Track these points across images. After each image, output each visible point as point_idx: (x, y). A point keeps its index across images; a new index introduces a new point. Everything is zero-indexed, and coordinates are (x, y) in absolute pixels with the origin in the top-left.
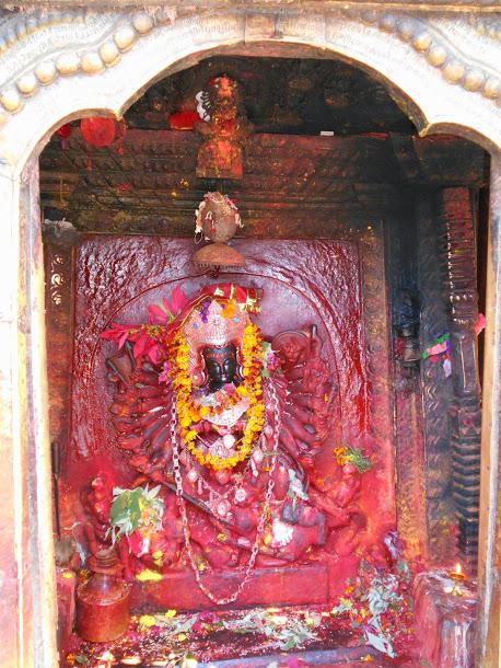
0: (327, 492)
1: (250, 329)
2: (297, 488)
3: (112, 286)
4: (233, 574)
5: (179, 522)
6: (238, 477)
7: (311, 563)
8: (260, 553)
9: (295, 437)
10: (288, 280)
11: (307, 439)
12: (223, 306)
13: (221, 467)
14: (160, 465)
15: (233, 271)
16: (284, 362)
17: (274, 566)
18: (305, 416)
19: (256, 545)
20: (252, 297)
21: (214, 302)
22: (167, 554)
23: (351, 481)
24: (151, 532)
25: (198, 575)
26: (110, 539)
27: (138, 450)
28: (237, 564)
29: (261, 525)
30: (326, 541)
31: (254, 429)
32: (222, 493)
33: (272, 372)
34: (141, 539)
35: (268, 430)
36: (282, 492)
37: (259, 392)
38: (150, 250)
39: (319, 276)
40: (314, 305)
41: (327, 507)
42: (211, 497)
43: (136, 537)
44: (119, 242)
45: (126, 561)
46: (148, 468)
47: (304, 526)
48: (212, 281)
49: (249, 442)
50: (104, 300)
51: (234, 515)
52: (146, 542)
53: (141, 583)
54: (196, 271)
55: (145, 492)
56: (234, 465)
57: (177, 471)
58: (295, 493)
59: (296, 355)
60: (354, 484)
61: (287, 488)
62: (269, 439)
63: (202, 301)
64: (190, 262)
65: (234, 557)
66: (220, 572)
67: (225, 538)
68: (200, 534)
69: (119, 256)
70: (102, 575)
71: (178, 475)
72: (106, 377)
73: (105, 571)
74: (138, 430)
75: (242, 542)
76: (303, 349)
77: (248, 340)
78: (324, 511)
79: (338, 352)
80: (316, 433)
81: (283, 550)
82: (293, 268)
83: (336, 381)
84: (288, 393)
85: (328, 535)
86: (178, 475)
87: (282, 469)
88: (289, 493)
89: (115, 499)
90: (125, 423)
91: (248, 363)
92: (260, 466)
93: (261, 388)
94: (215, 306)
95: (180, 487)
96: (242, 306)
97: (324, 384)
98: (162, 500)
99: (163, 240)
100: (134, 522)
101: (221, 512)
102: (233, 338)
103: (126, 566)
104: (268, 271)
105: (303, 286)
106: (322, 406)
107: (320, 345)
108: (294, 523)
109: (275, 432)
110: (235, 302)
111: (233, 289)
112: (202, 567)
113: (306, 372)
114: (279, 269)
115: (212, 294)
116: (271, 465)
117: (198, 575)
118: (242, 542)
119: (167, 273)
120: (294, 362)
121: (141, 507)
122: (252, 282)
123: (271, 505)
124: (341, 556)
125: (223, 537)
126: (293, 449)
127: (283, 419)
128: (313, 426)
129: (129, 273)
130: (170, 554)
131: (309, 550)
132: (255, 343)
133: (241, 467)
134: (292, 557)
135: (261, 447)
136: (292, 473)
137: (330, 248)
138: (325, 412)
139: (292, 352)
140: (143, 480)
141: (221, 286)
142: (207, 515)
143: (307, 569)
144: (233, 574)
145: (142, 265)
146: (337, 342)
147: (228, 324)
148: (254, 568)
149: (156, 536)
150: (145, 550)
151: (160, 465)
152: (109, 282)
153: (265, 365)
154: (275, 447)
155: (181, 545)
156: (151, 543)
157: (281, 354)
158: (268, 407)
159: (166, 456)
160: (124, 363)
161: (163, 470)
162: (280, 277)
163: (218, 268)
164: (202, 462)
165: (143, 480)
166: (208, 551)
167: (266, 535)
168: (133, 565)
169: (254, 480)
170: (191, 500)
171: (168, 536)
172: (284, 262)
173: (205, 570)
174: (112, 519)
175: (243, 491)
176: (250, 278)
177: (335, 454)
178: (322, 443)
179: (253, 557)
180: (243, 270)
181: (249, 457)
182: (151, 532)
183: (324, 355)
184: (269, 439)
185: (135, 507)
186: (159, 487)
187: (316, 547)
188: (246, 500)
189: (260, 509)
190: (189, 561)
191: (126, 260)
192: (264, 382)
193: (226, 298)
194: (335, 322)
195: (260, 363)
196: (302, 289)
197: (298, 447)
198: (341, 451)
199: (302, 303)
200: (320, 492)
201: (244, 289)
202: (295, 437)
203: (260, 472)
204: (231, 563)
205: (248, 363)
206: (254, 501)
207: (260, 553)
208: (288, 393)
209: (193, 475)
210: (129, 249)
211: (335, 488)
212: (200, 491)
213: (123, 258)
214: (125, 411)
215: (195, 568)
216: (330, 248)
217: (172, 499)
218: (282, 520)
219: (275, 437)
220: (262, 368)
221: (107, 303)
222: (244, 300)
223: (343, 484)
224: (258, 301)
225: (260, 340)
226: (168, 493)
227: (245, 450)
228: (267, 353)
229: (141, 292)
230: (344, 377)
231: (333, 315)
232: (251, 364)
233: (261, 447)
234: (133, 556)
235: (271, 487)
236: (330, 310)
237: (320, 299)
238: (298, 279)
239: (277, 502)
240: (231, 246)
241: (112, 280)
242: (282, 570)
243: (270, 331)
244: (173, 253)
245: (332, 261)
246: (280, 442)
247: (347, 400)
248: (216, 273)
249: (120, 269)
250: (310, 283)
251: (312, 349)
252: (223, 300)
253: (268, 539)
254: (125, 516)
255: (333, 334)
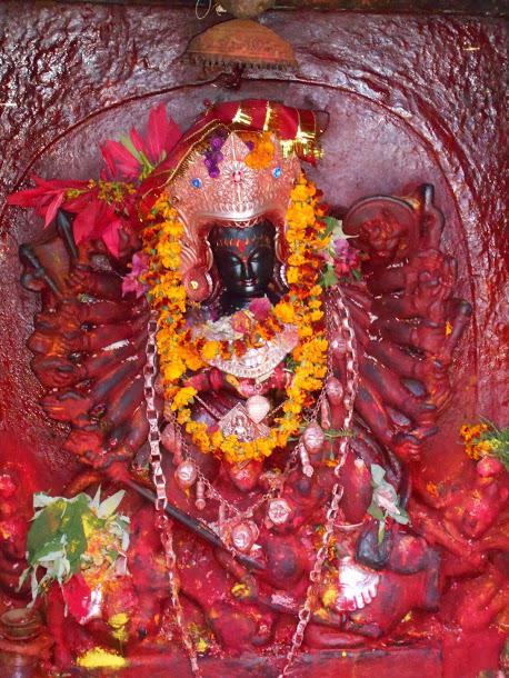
0: (442, 510)
1: (301, 191)
2: (387, 500)
3: (31, 104)
4: (261, 659)
5: (160, 561)
6: (273, 478)
7: (411, 643)
8: (314, 622)
9: (387, 402)
10: (377, 95)
11: (411, 405)
12: (250, 145)
13: (241, 457)
14: (124, 452)
15: (269, 75)
16: (365, 256)
17: (339, 647)
18: (406, 364)
19: (306, 607)
20: (306, 128)
21: (232, 137)
22: (137, 619)
23: (492, 490)
24: (105, 577)
25: (194, 660)
26: (27, 590)
27: (81, 423)
28: (270, 641)
29: (316, 569)
30: (441, 601)
31: (307, 386)
32: (243, 508)
33: (343, 277)
34: (87, 591)
35: (334, 389)
36: (358, 507)
37: (317, 315)
38: (105, 32)
39: (439, 88)
40: (429, 146)
41: (441, 534)
42: (222, 514)
43: (78, 587)
44: (44, 14)
45: (57, 631)
46: (101, 457)
47: (400, 573)
48: (226, 100)
49: (297, 409)
50: (16, 132)
51: (264, 550)
52: (97, 595)
53: (86, 672)
54: (197, 71)
55: (94, 503)
56: (268, 453)
57: (157, 465)
58: (383, 510)
59: (392, 244)
60: (498, 495)
61: (368, 500)
62: (336, 407)
63: (210, 131)
64: (187, 57)
65: (263, 628)
66: (237, 656)
67: (247, 593)
68: (199, 584)
69: (46, 43)
70: (13, 654)
71: (158, 471)
72: (20, 282)
73: (18, 649)
74: (78, 383)
75: (279, 599)
76: (404, 233)
77: (299, 214)
78: (438, 545)
79: (473, 239)
80: (427, 396)
81: (358, 617)
82: (389, 73)
83: (467, 297)
84: (374, 318)
85: (445, 591)
86: (158, 471)
87: (359, 463)
88: (371, 510)
89: (37, 514)
90: (58, 370)
91: (297, 258)
92: (317, 458)
93: (322, 308)
94: (234, 146)
95: (162, 495)
96: (287, 145)
97: (445, 301)
98: (127, 519)
99: (131, 12)
100: (74, 559)
101: (240, 543)
102: (270, 207)
103: (58, 640)
104: (339, 78)
105: (407, 107)
106: (440, 345)
107: (437, 225)
108: (378, 566)
109: (347, 393)
110: (273, 138)
111: (269, 110)
112: (202, 646)
113: (412, 277)
114: (360, 74)
115: (228, 121)
116: (338, 455)
117: (194, 660)
118: (279, 599)
119: (140, 80)
120: (387, 258)
121: (88, 530)
122: (308, 100)
123: (337, 532)
124: (470, 631)
125: (243, 590)
126: (380, 424)
127: (364, 369)
128: (422, 383)
129: (63, 77)
130: (142, 619)
131: (408, 618)
132: (312, 221)
133: (281, 458)
134: (373, 630)
135: (319, 421)
136: (378, 472)
137: (462, 33)
138: (445, 354)
139: (384, 238)
140: (91, 479)
141: (247, 106)
142: (213, 547)
143: (404, 653)
144: (261, 659)
145: (89, 61)
146: (471, 220)
147: (259, 181)
148: (301, 649)
149: (115, 586)
150: (95, 611)
151: (124, 452)
152: (26, 96)
153: (330, 263)
154: (347, 421)
155: (163, 604)
156: (105, 597)
157: (360, 240)
158: (335, 345)
159: (137, 435)
160: (56, 254)
161: (129, 462)
162: (362, 88)
163: (240, 69)
164: (206, 447)
165: (91, 479)
166: (214, 615)
167: (326, 588)
168: (71, 638)
169: (304, 484)
170: (183, 519)
171: (137, 586)
172: (370, 59)
173: (208, 650)
174: (33, 553)
175: (283, 503)
176: (303, 90)
177: (463, 438)
178: (436, 414)
179: (299, 628)
180: (289, 75)
181: (297, 437)
182: (105, 577)
183: (446, 246)
184: (336, 407)
185: (75, 530)
186: (120, 495)
187: (422, 613)
188: (290, 520)
189: (315, 538)
190: (177, 633)
191: (58, 52)
192: (327, 296)
193: (255, 128)
194: (469, 180)
195: (321, 258)
196: (406, 114)
197: (391, 424)
198: (475, 430)
199: (404, 142)
200: (431, 509)
201: (291, 111)
202: (386, 402)
203: (316, 468)
204: (257, 639)
205: (297, 258)
206: (304, 523)
207: (314, 622)
208: (374, 318)
209: (186, 472)
210: (65, 30)
211: (460, 503)
212: (200, 503)
213: (53, 48)
214: (57, 348)
215: (189, 646)
216: (462, 33)
217: (146, 515)
218: (359, 560)
219: (347, 401)
220: (325, 268)
221: (20, 138)
222: (291, 135)
223: (477, 493)
224: (318, 136)
225: (321, 213)
226: (139, 505)
227: (288, 425)
228: (335, 239)
229: (90, 115)
230: (484, 288)
231: (466, 166)
232: (302, 260)
233: (319, 421)
234: (72, 622)
235: (337, 497)
236: (461, 155)
237: (440, 134)
238: (398, 94)
239: (348, 527)
240: (269, 26)
241: (31, 90)
242: (355, 655)
243: (340, 197)
244: (152, 38)
245: (466, 58)
246: (356, 411)
247: (489, 334)
248: (236, 77)
249: (47, 69)
250: (420, 100)
251: (424, 234)
252: (250, 132)
253: (329, 596)
254: (57, 547)
255: (464, 205)
